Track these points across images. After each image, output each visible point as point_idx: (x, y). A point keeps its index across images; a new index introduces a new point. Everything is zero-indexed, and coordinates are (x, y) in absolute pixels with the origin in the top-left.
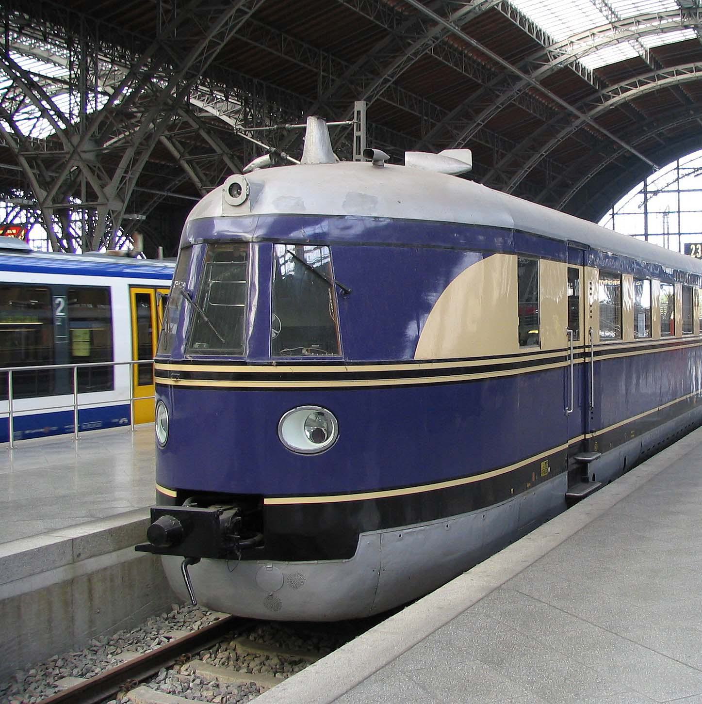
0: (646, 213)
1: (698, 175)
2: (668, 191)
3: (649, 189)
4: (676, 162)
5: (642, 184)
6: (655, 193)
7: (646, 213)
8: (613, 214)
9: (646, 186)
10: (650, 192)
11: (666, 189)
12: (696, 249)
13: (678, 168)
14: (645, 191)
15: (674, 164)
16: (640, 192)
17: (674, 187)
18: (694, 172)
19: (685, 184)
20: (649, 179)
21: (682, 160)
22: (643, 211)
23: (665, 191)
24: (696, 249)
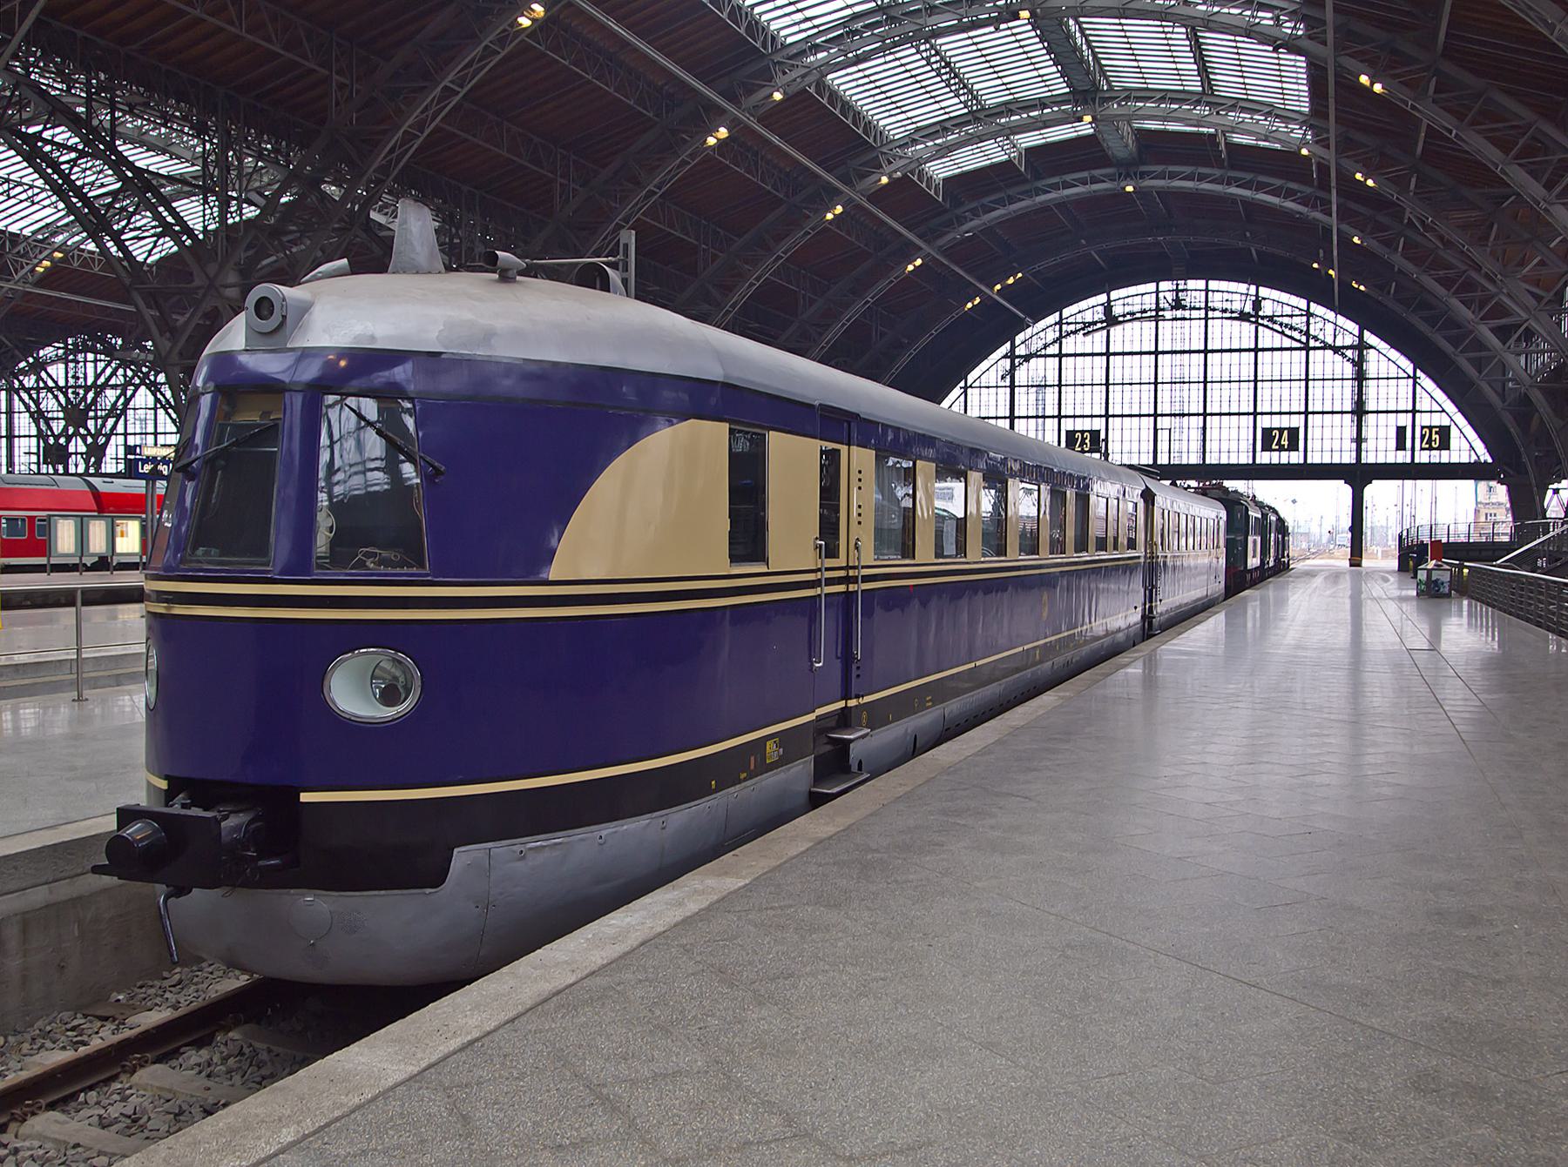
0: (1012, 387)
1: (1089, 332)
2: (1046, 356)
3: (1018, 352)
4: (1058, 313)
5: (1008, 345)
6: (1027, 358)
7: (1012, 387)
8: (966, 388)
9: (1013, 347)
10: (1020, 357)
11: (1043, 352)
12: (1083, 439)
13: (1060, 323)
14: (1011, 355)
15: (1054, 318)
16: (1005, 357)
17: (1054, 349)
18: (1083, 329)
19: (1069, 345)
20: (1019, 338)
21: (1066, 312)
22: (1008, 384)
23: (1041, 356)
24: (1083, 439)
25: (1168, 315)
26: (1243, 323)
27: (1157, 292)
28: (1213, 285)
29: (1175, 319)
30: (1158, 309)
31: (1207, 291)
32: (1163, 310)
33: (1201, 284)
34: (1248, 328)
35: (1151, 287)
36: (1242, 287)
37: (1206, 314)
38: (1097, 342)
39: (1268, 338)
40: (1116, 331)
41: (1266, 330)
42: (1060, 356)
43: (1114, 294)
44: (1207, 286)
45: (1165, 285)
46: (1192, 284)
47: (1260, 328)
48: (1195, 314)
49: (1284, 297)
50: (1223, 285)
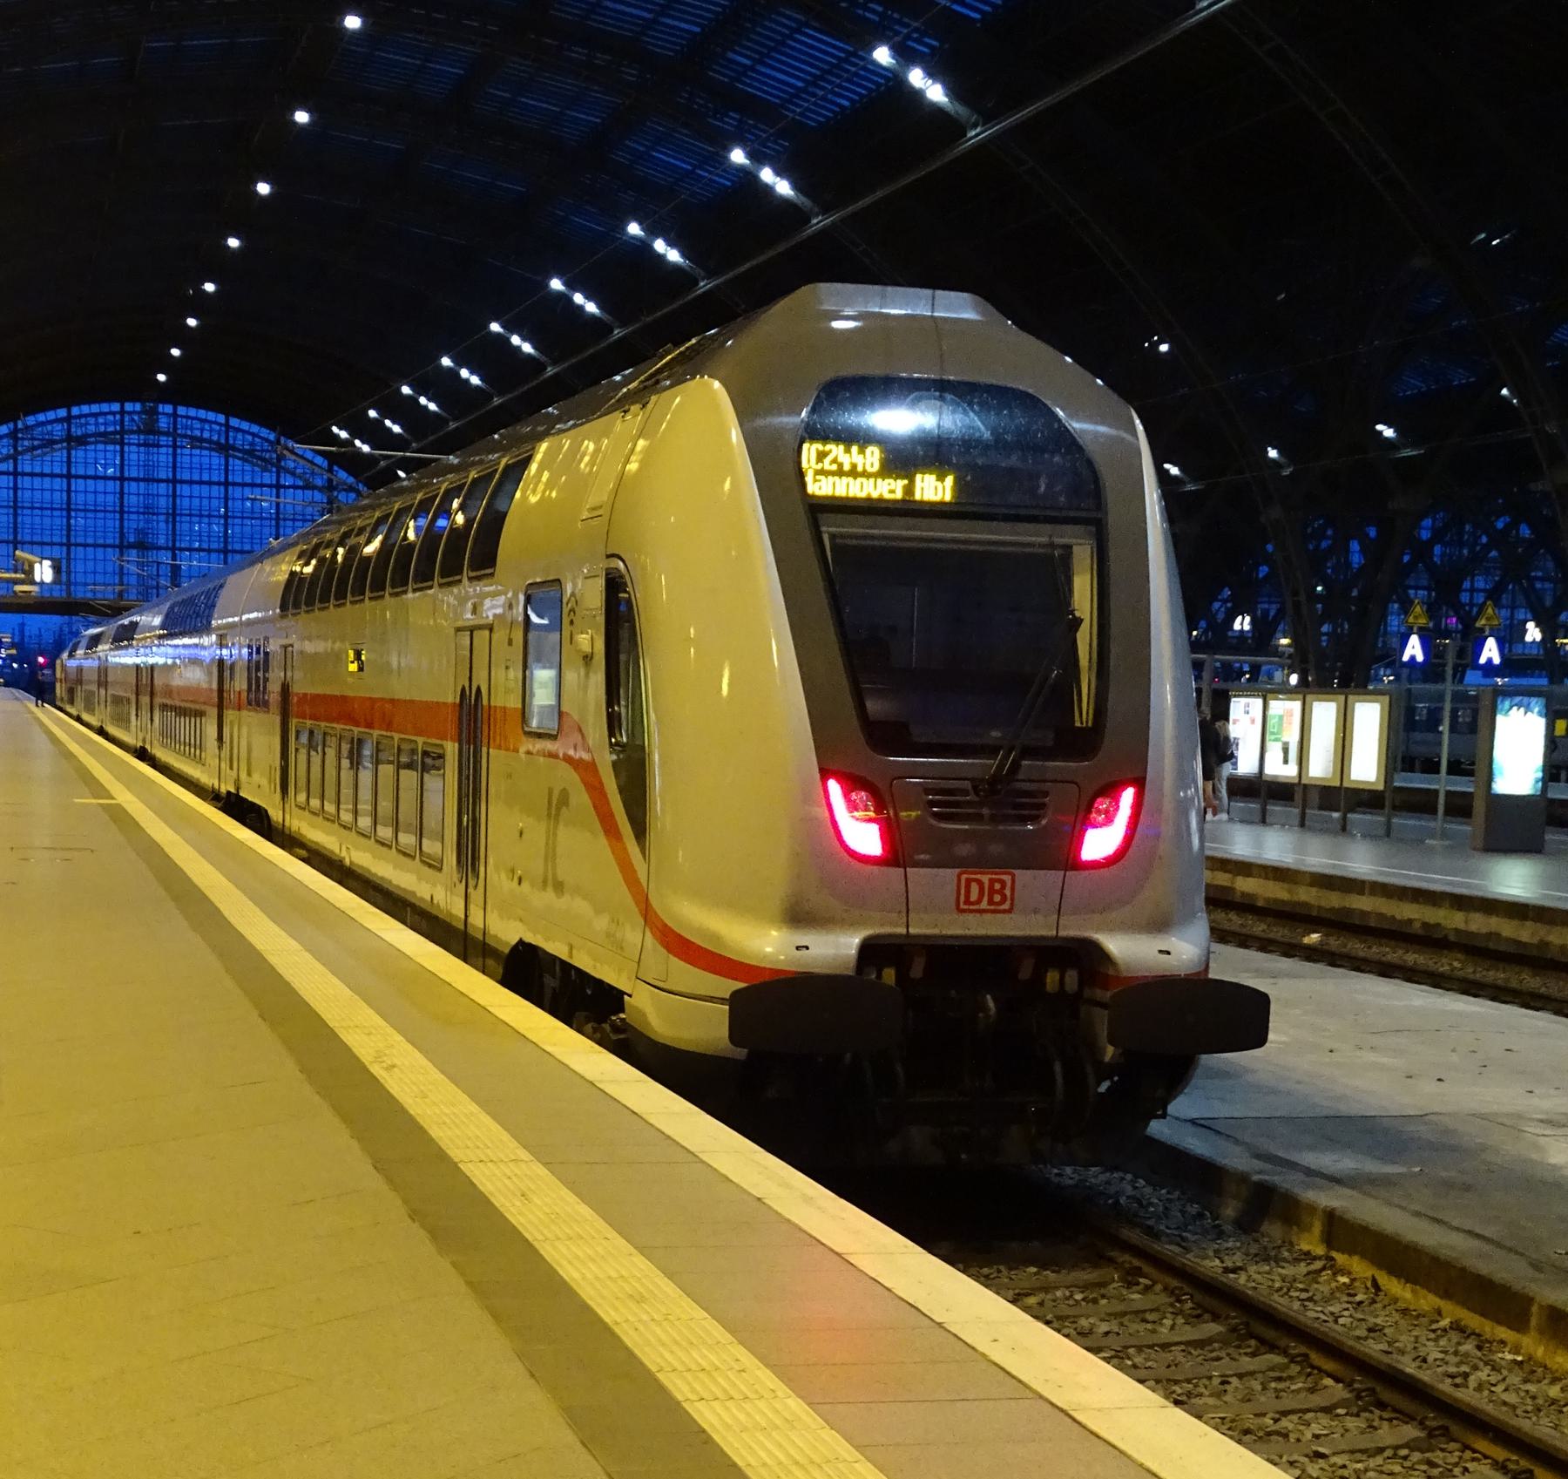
25: (134, 438)
26: (213, 453)
27: (122, 412)
28: (181, 410)
29: (139, 445)
30: (122, 432)
31: (175, 415)
32: (132, 432)
33: (168, 409)
34: (217, 460)
35: (116, 407)
36: (211, 416)
37: (175, 441)
38: (55, 460)
39: (241, 470)
40: (78, 454)
41: (238, 462)
42: (15, 474)
43: (75, 411)
44: (175, 410)
45: (129, 407)
46: (161, 408)
47: (231, 460)
48: (163, 440)
49: (255, 429)
50: (192, 412)
